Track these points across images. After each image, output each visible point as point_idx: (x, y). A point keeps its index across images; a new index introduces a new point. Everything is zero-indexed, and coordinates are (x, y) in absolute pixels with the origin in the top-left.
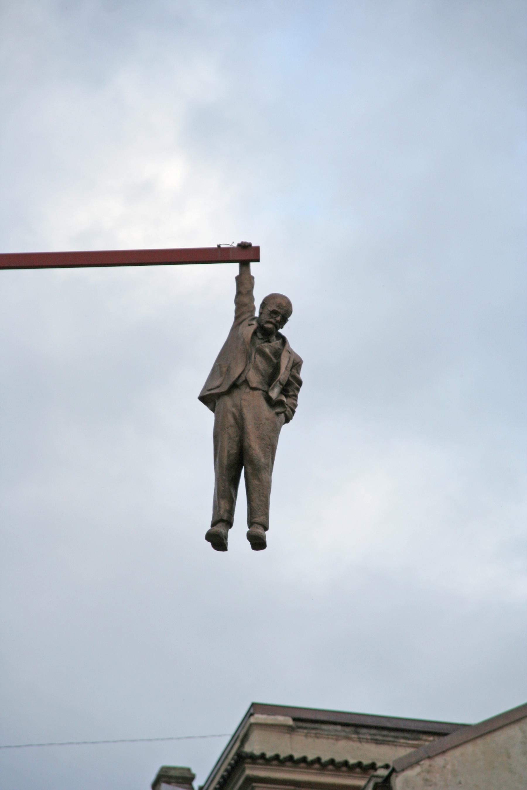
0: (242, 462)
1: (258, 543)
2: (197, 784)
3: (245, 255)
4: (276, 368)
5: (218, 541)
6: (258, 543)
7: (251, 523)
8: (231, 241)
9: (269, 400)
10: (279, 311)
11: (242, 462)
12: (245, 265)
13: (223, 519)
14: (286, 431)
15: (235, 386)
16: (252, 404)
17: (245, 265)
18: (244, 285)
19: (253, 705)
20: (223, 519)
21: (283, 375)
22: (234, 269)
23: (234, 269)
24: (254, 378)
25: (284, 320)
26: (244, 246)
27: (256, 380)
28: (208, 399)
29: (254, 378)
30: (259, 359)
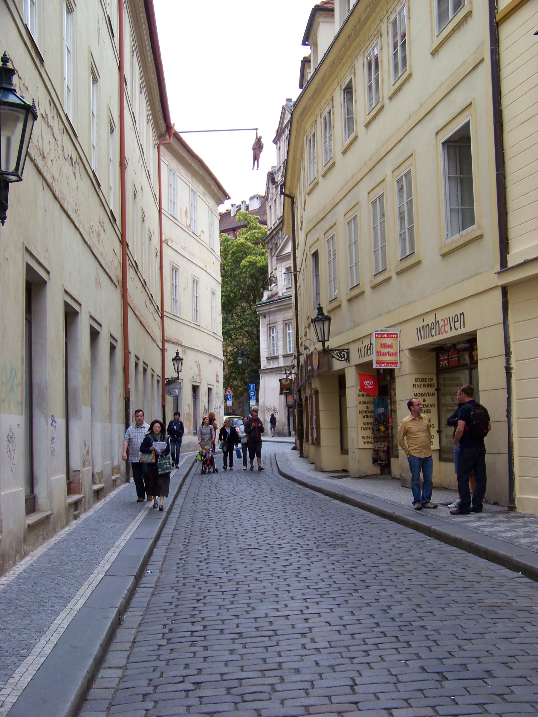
0: (256, 158)
3: (257, 129)
10: (260, 138)
11: (256, 158)
14: (261, 154)
20: (254, 166)
24: (257, 147)
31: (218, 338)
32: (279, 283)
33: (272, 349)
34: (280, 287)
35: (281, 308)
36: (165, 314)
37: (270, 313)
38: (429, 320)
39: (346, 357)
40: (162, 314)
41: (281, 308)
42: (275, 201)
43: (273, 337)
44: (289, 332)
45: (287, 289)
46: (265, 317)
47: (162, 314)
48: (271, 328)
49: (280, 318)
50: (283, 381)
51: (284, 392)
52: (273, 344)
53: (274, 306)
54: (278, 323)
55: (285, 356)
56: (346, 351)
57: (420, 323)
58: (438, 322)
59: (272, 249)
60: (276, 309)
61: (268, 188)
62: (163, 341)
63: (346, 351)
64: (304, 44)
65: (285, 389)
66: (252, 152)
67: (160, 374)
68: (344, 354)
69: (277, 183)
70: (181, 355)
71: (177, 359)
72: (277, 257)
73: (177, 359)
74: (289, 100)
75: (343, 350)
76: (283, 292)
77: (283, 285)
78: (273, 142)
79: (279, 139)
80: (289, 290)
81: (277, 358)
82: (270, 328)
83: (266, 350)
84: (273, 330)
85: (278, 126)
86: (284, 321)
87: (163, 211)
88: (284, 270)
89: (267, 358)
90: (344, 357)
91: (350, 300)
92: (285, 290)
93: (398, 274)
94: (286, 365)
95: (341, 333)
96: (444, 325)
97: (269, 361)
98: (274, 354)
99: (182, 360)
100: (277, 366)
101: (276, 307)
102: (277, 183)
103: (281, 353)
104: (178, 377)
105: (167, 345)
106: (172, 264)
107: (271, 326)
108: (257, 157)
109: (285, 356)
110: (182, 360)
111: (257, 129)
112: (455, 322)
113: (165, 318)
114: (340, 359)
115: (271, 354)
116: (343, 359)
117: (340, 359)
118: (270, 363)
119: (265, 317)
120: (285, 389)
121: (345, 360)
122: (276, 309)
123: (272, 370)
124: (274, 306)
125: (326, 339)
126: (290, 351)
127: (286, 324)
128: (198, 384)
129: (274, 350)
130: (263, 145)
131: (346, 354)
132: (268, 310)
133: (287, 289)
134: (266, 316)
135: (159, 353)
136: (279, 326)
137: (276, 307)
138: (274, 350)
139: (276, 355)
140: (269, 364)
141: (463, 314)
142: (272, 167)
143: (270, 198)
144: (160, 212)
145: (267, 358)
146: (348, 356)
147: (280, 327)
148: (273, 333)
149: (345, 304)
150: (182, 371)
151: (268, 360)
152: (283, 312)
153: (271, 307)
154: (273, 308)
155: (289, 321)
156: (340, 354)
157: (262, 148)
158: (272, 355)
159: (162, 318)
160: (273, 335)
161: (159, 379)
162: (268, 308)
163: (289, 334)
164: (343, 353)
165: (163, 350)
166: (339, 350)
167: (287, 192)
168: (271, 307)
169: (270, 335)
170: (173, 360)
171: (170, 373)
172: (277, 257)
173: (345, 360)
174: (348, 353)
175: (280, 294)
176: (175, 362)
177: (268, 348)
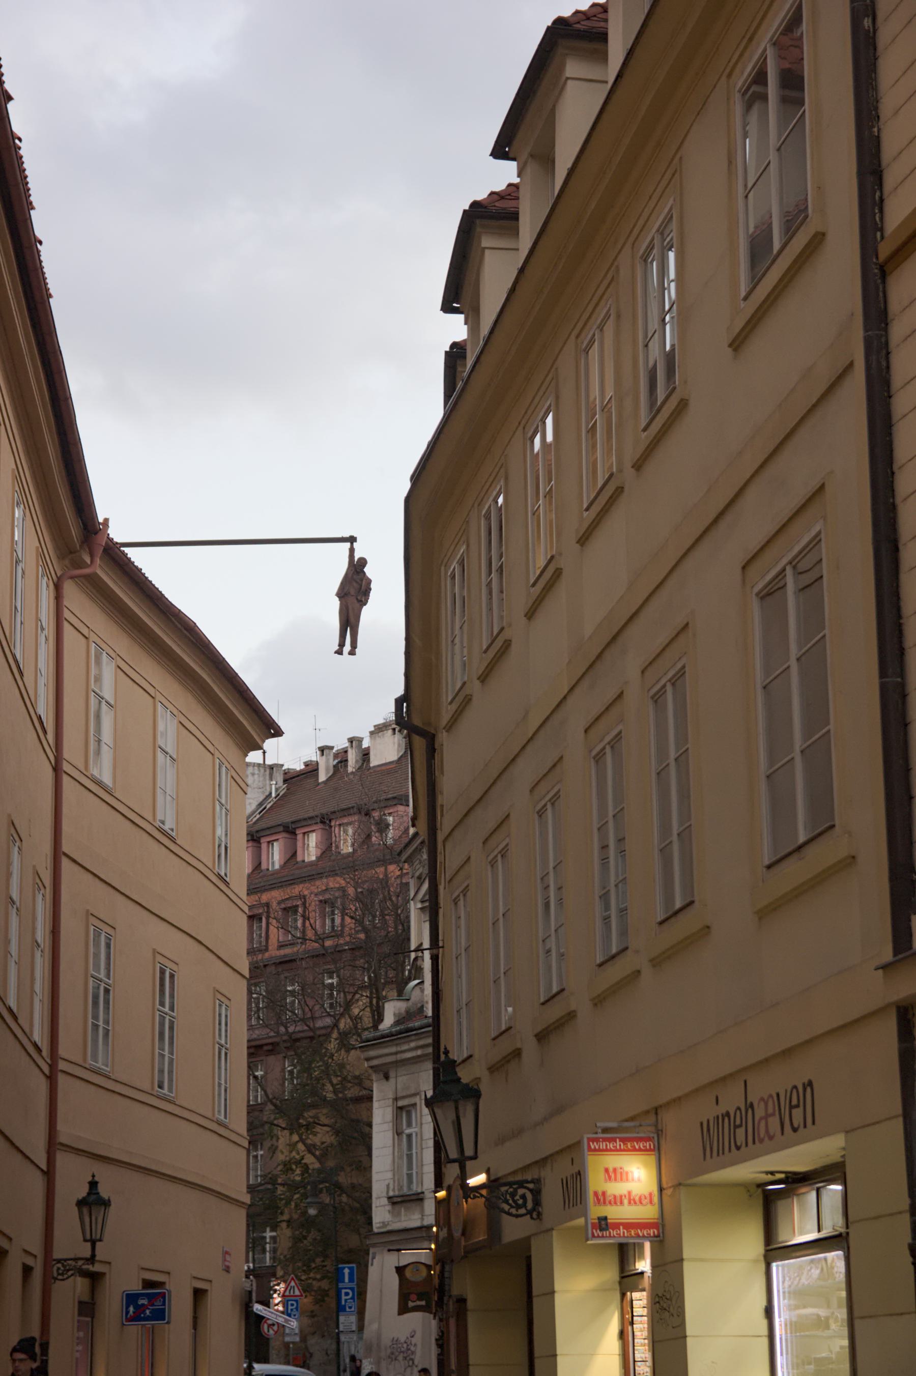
3: (352, 540)
5: (339, 652)
8: (346, 535)
10: (363, 562)
12: (352, 544)
13: (342, 644)
16: (352, 601)
17: (352, 544)
18: (352, 551)
20: (342, 644)
21: (363, 588)
23: (348, 545)
24: (352, 592)
25: (364, 566)
29: (352, 592)
30: (355, 584)
31: (233, 1137)
33: (405, 1171)
36: (62, 1065)
38: (732, 1099)
39: (530, 1205)
40: (53, 1066)
43: (409, 1136)
46: (387, 1078)
47: (53, 1066)
50: (408, 1273)
51: (411, 1304)
53: (413, 1045)
56: (531, 1186)
57: (707, 1110)
58: (752, 1106)
60: (419, 1052)
62: (53, 1145)
63: (531, 1186)
64: (447, 307)
65: (413, 1297)
66: (336, 603)
67: (35, 1245)
68: (523, 1197)
70: (104, 1191)
71: (93, 1201)
73: (93, 1201)
75: (521, 1184)
81: (418, 1199)
83: (389, 1175)
84: (409, 1114)
87: (66, 767)
90: (524, 1205)
91: (542, 1037)
93: (657, 962)
95: (518, 1132)
96: (767, 1117)
97: (397, 1207)
98: (409, 1188)
99: (106, 1203)
100: (417, 1224)
101: (417, 1048)
105: (62, 1159)
106: (93, 920)
107: (400, 1103)
108: (352, 619)
110: (106, 1203)
112: (791, 1107)
113: (61, 1079)
114: (513, 1211)
115: (401, 1188)
116: (522, 1211)
117: (513, 1211)
118: (399, 1214)
119: (387, 1078)
120: (413, 1297)
121: (530, 1213)
122: (419, 1052)
124: (413, 1045)
125: (469, 1152)
129: (410, 1176)
130: (369, 582)
131: (529, 1196)
134: (392, 1074)
135: (37, 1183)
137: (417, 1048)
138: (410, 1176)
139: (415, 1188)
141: (810, 1084)
144: (57, 769)
145: (389, 1198)
146: (537, 1203)
148: (409, 1125)
149: (530, 1048)
150: (106, 1237)
151: (394, 1204)
153: (405, 1047)
156: (513, 1195)
158: (405, 1191)
159: (52, 1079)
160: (408, 1131)
161: (30, 1261)
162: (393, 1049)
164: (521, 1191)
165: (49, 1174)
166: (510, 1184)
167: (417, 721)
168: (405, 1047)
170: (81, 1203)
171: (69, 1242)
173: (530, 1213)
174: (536, 1193)
176: (85, 1210)
177: (395, 1170)
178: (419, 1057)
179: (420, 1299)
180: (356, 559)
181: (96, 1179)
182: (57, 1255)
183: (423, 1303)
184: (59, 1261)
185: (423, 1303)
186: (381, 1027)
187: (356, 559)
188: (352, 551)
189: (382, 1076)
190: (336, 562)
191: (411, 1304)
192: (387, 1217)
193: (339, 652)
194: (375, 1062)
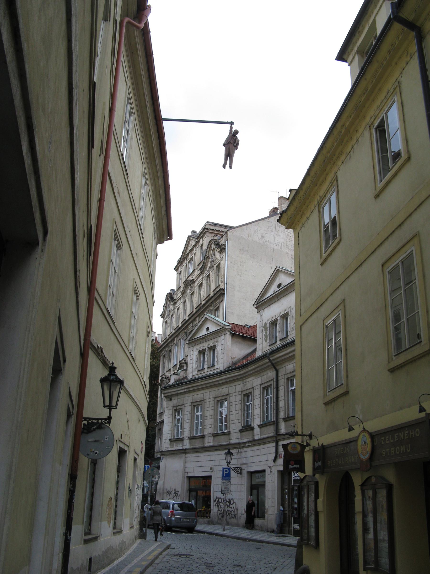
1: (231, 167)
2: (197, 233)
3: (232, 123)
4: (236, 141)
5: (224, 167)
6: (231, 167)
7: (230, 164)
8: (230, 121)
9: (234, 146)
10: (236, 132)
12: (231, 125)
14: (236, 151)
15: (229, 143)
17: (231, 125)
18: (231, 128)
19: (207, 222)
21: (236, 143)
22: (230, 125)
23: (230, 125)
24: (232, 142)
26: (232, 122)
27: (232, 144)
28: (224, 145)
29: (232, 142)
32: (190, 366)
33: (176, 431)
34: (190, 370)
35: (191, 389)
37: (178, 394)
41: (191, 389)
42: (172, 315)
43: (178, 420)
44: (197, 414)
45: (198, 371)
48: (177, 410)
49: (188, 400)
50: (289, 448)
51: (291, 467)
52: (178, 426)
54: (186, 405)
55: (190, 438)
59: (164, 356)
61: (165, 306)
65: (292, 462)
66: (223, 149)
69: (176, 300)
72: (189, 341)
74: (194, 232)
76: (194, 374)
77: (194, 367)
78: (174, 269)
79: (180, 265)
80: (200, 372)
81: (182, 440)
82: (175, 410)
84: (179, 412)
85: (181, 254)
86: (192, 403)
88: (196, 353)
89: (170, 439)
92: (195, 373)
94: (192, 447)
97: (172, 443)
98: (178, 436)
100: (181, 448)
101: (184, 389)
102: (176, 300)
103: (186, 434)
104: (110, 418)
108: (231, 152)
109: (190, 438)
111: (232, 123)
115: (174, 436)
118: (173, 445)
120: (292, 462)
122: (185, 390)
123: (175, 452)
126: (197, 433)
127: (194, 406)
128: (126, 448)
130: (239, 141)
132: (177, 392)
133: (198, 371)
134: (173, 398)
136: (186, 408)
137: (184, 389)
140: (171, 445)
142: (171, 290)
143: (166, 315)
145: (170, 439)
147: (187, 409)
152: (192, 394)
154: (181, 389)
155: (199, 403)
157: (238, 144)
158: (176, 437)
160: (178, 418)
163: (197, 416)
169: (175, 418)
172: (189, 341)
175: (190, 377)
177: (172, 430)
178: (185, 392)
179: (296, 464)
180: (233, 131)
181: (114, 365)
182: (85, 416)
183: (298, 466)
184: (85, 419)
185: (298, 466)
186: (169, 384)
187: (233, 131)
188: (231, 128)
189: (169, 399)
190: (225, 131)
191: (291, 467)
192: (168, 446)
193: (224, 167)
194: (167, 395)
